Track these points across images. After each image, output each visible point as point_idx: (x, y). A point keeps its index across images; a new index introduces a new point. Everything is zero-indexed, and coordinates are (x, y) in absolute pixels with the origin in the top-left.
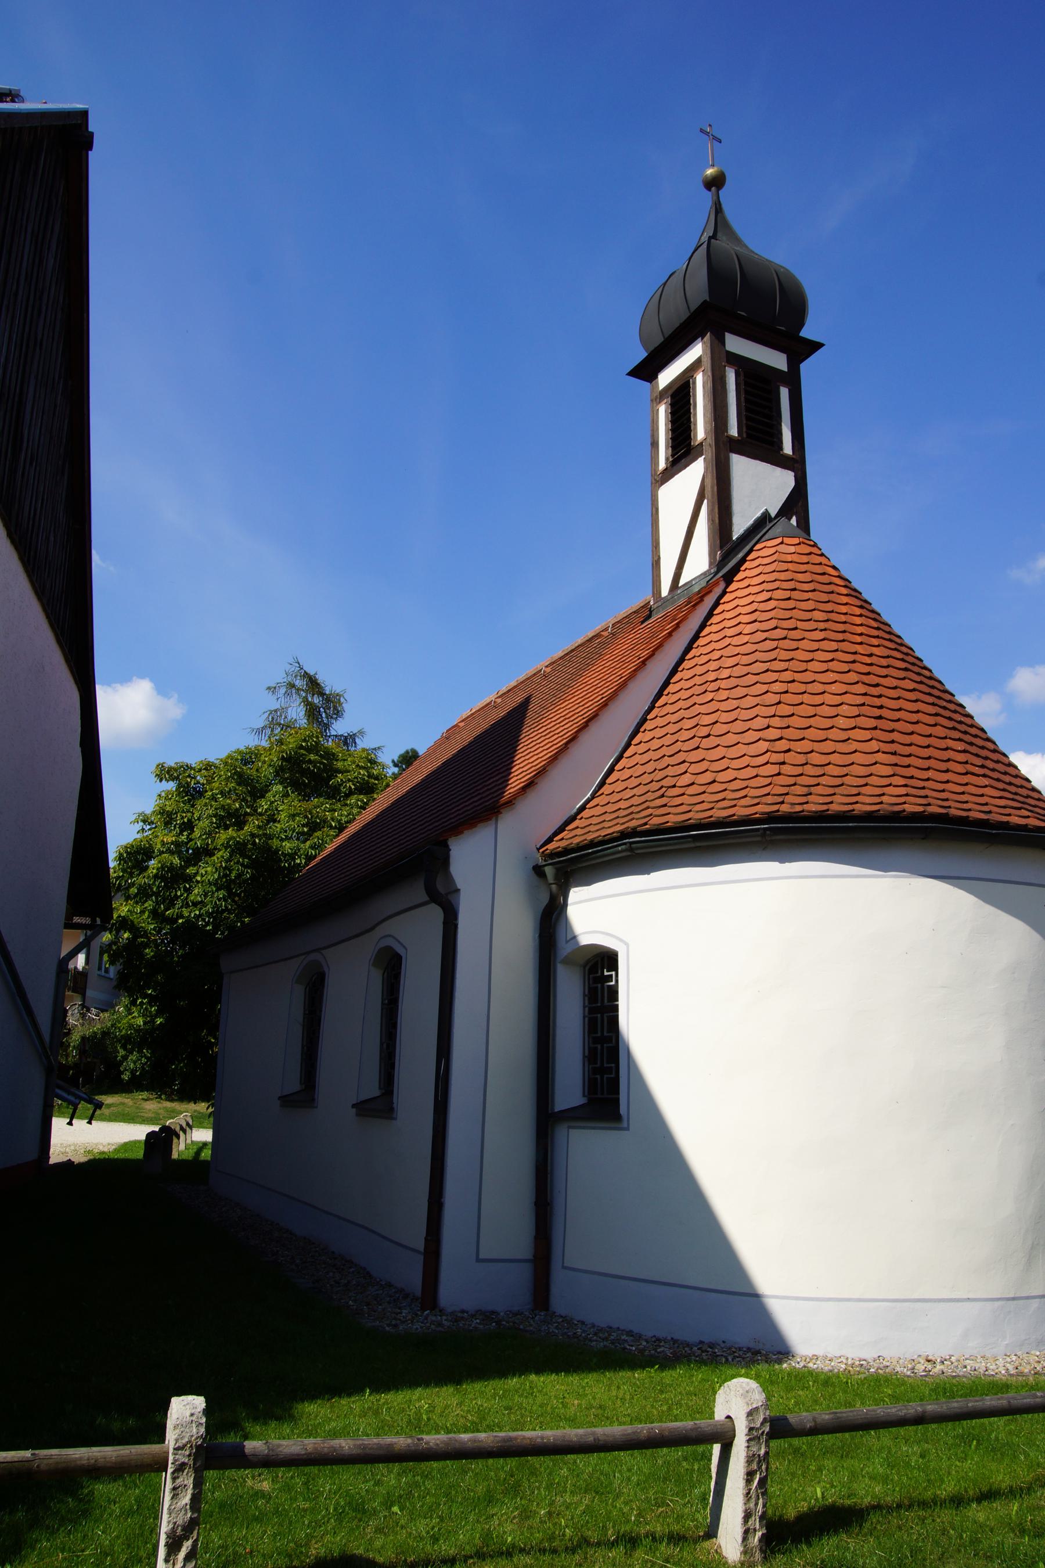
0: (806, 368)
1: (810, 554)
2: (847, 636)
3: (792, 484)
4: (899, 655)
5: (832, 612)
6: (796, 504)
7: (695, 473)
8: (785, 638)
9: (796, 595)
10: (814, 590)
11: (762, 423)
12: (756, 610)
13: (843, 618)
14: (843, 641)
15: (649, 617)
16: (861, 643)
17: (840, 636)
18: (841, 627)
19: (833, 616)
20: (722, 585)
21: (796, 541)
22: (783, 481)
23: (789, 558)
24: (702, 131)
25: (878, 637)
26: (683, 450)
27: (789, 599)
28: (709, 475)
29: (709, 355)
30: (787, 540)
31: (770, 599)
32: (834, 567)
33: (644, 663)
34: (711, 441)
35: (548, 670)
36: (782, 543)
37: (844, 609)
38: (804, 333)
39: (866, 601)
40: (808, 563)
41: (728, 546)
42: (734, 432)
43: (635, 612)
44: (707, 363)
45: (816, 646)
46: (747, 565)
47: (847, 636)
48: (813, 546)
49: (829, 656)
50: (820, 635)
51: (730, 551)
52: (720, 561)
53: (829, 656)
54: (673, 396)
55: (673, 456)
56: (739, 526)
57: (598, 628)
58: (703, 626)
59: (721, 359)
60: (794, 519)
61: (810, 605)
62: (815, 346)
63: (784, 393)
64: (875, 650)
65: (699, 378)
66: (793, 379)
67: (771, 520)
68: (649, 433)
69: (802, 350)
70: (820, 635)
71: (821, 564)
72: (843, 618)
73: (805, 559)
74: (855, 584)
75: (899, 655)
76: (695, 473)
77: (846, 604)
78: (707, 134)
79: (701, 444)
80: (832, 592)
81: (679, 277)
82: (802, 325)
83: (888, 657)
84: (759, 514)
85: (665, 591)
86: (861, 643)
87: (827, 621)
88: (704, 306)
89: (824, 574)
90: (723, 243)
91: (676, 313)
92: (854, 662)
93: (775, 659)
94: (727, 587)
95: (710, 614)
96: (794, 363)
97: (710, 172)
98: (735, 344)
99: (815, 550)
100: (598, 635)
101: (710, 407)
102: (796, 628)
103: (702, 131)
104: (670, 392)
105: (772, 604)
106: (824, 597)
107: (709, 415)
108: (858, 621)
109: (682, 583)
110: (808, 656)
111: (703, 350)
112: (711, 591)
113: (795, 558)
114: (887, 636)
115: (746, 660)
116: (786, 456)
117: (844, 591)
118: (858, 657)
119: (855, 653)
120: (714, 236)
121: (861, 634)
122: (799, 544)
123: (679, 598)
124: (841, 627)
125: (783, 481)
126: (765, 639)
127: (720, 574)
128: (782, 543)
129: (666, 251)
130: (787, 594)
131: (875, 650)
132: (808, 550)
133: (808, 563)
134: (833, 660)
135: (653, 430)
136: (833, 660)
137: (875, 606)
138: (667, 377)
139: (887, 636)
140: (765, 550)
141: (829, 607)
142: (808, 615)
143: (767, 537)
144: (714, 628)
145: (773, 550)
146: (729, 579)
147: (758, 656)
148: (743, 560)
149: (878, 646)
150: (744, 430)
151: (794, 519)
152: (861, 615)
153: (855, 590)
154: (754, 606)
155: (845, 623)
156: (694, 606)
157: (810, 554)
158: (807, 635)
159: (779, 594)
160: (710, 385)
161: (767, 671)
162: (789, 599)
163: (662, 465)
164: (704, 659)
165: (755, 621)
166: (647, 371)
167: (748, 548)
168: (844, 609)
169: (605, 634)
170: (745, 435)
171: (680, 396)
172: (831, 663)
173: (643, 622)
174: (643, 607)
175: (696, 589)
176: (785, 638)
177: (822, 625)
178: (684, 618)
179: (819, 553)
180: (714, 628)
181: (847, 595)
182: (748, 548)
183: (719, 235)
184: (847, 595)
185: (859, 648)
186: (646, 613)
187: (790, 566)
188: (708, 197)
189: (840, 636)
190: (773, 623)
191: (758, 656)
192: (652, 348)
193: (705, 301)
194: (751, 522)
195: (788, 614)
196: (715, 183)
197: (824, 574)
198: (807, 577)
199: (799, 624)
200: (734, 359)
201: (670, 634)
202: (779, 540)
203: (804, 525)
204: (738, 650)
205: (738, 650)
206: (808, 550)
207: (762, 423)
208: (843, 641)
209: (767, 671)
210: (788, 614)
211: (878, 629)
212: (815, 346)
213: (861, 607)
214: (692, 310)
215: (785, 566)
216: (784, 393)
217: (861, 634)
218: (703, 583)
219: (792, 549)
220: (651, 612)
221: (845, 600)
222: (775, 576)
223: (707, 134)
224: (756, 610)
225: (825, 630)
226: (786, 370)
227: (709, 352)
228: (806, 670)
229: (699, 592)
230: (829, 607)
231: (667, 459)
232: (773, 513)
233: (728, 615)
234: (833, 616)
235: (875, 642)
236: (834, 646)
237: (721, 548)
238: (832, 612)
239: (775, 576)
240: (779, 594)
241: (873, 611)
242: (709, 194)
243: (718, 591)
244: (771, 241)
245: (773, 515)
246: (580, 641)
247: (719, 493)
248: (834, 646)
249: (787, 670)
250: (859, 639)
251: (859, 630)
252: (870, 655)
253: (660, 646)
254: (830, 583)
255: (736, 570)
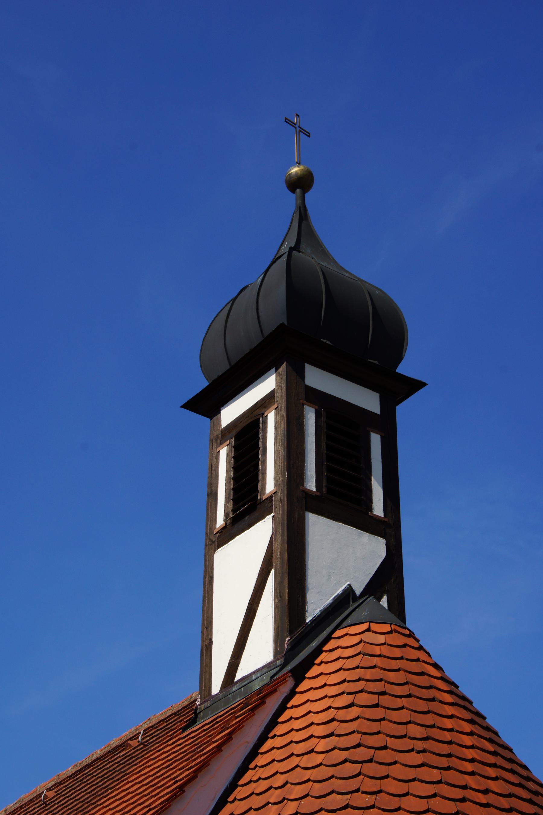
0: (404, 411)
1: (405, 646)
2: (454, 762)
3: (382, 553)
4: (525, 794)
5: (433, 726)
6: (388, 579)
7: (259, 536)
8: (370, 761)
9: (385, 700)
10: (409, 696)
11: (347, 477)
12: (333, 720)
13: (448, 736)
14: (449, 768)
15: (193, 722)
16: (472, 773)
17: (444, 762)
18: (445, 749)
19: (435, 733)
20: (290, 682)
21: (386, 628)
22: (370, 551)
23: (377, 650)
24: (287, 121)
25: (494, 766)
26: (246, 507)
27: (376, 706)
28: (279, 539)
29: (284, 389)
30: (375, 627)
31: (351, 705)
32: (436, 666)
33: (181, 789)
34: (282, 495)
35: (51, 794)
36: (368, 630)
37: (448, 724)
38: (402, 369)
39: (478, 714)
40: (401, 658)
41: (300, 630)
42: (311, 485)
43: (175, 714)
44: (281, 399)
45: (411, 773)
46: (323, 657)
47: (454, 762)
48: (408, 636)
49: (430, 790)
50: (418, 759)
51: (302, 637)
52: (289, 651)
53: (430, 790)
54: (237, 437)
55: (234, 511)
56: (316, 604)
57: (126, 734)
58: (263, 738)
59: (297, 395)
60: (385, 598)
61: (404, 715)
62: (414, 386)
63: (376, 440)
64: (493, 785)
65: (271, 417)
66: (386, 424)
67: (355, 598)
68: (206, 481)
69: (399, 390)
70: (418, 759)
71: (418, 660)
72: (448, 736)
73: (397, 653)
74: (464, 690)
75: (525, 794)
76: (259, 536)
77: (452, 717)
78: (293, 125)
79: (270, 498)
80: (433, 700)
81: (251, 293)
82: (399, 358)
83: (510, 795)
84: (340, 591)
85: (216, 688)
86: (472, 773)
87: (427, 738)
88: (280, 331)
89: (422, 674)
90: (306, 256)
91: (246, 335)
92: (463, 800)
93: (357, 791)
94: (297, 685)
95: (273, 723)
96: (389, 404)
97: (295, 170)
98: (317, 378)
99: (410, 641)
100: (124, 745)
101: (282, 453)
102: (385, 748)
103: (287, 121)
104: (234, 432)
105: (355, 712)
106: (423, 706)
107: (281, 463)
108: (468, 741)
109: (239, 675)
110: (402, 788)
111: (277, 383)
112: (275, 691)
113: (385, 651)
114: (508, 765)
115: (318, 790)
116: (376, 519)
117: (449, 698)
118: (469, 794)
119: (465, 787)
120: (297, 247)
121: (472, 761)
122: (390, 632)
123: (234, 698)
124: (445, 749)
125: (370, 551)
126: (345, 761)
127: (288, 668)
128: (368, 630)
129: (235, 261)
130: (374, 699)
131: (493, 785)
132: (402, 640)
133: (401, 658)
134: (434, 795)
135: (210, 478)
136: (434, 795)
137: (491, 721)
138: (230, 413)
139: (508, 765)
140: (347, 639)
141: (429, 719)
142: (401, 730)
143: (349, 621)
144: (278, 742)
145: (356, 639)
146: (299, 674)
147: (335, 784)
148: (318, 651)
149: (496, 779)
150: (325, 483)
151: (385, 598)
152: (471, 734)
153: (464, 698)
154: (332, 713)
155: (450, 743)
156: (253, 710)
157: (405, 646)
158: (401, 757)
159: (363, 699)
160: (283, 426)
161: (346, 807)
162: (376, 706)
163: (220, 521)
164: (263, 786)
165: (332, 734)
166: (207, 403)
167: (325, 634)
168: (448, 724)
169: (134, 743)
170: (325, 490)
171: (246, 437)
172: (432, 801)
173: (184, 729)
174: (186, 707)
175: (257, 686)
176: (370, 761)
177: (420, 745)
178: (240, 726)
179: (416, 645)
180: (278, 742)
181: (452, 704)
182: (325, 634)
183: (303, 246)
184: (452, 704)
185: (470, 781)
186: (189, 715)
187: (378, 661)
188: (290, 201)
189: (444, 762)
190: (355, 739)
191: (335, 784)
192: (215, 377)
193: (282, 325)
194: (330, 600)
195: (374, 727)
196: (301, 184)
197: (422, 674)
198: (400, 677)
199: (390, 742)
200: (316, 397)
201: (219, 749)
202: (365, 626)
203: (398, 608)
204: (308, 774)
205: (308, 774)
206: (402, 640)
207: (347, 477)
208: (449, 768)
209: (346, 807)
210: (374, 727)
211: (495, 754)
212: (414, 386)
213: (472, 722)
214: (267, 332)
215: (371, 661)
216: (376, 440)
217: (472, 761)
218: (266, 679)
219: (381, 639)
220: (196, 714)
221: (450, 710)
222: (359, 673)
223: (293, 125)
224: (333, 720)
225: (424, 751)
226: (377, 411)
227: (284, 386)
228: (399, 809)
229: (260, 691)
230: (429, 719)
231: (226, 515)
232: (358, 590)
233: (297, 724)
234: (435, 733)
235: (492, 772)
236: (436, 775)
237: (291, 633)
238: (433, 726)
239: (359, 673)
240: (363, 699)
241: (488, 729)
242: (293, 196)
243: (285, 690)
244: (363, 256)
245: (358, 592)
246: (99, 753)
247: (289, 563)
248: (436, 775)
249: (372, 807)
250: (469, 767)
251: (470, 754)
252: (486, 792)
253: (205, 765)
254: (430, 687)
255: (309, 663)
